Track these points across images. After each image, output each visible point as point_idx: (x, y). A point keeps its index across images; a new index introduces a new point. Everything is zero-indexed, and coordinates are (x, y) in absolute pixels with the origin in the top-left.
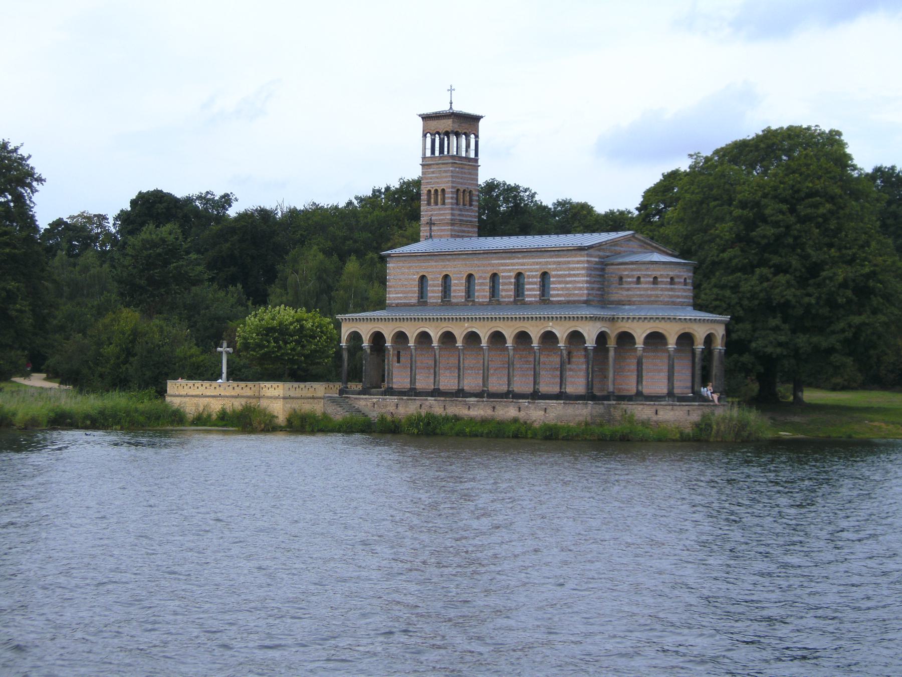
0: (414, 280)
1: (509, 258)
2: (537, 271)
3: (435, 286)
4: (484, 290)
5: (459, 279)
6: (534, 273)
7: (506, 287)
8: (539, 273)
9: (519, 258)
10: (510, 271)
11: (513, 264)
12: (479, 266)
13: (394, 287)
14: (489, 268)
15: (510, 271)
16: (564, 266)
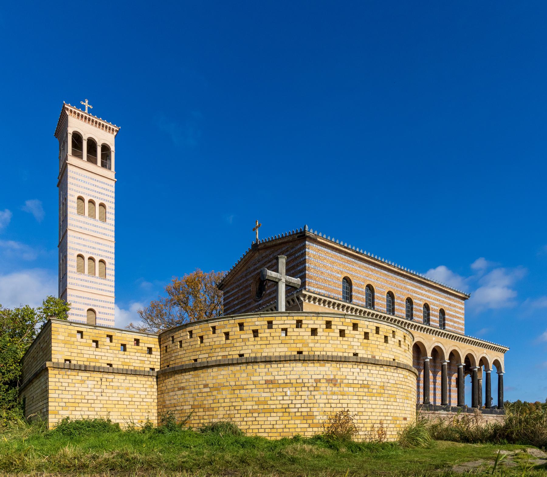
0: (338, 279)
1: (420, 288)
2: (437, 307)
3: (359, 293)
4: (402, 310)
5: (381, 293)
6: (436, 308)
7: (418, 313)
8: (439, 309)
9: (426, 291)
10: (420, 300)
11: (421, 294)
12: (397, 287)
13: (315, 280)
14: (405, 292)
15: (420, 300)
16: (453, 308)
